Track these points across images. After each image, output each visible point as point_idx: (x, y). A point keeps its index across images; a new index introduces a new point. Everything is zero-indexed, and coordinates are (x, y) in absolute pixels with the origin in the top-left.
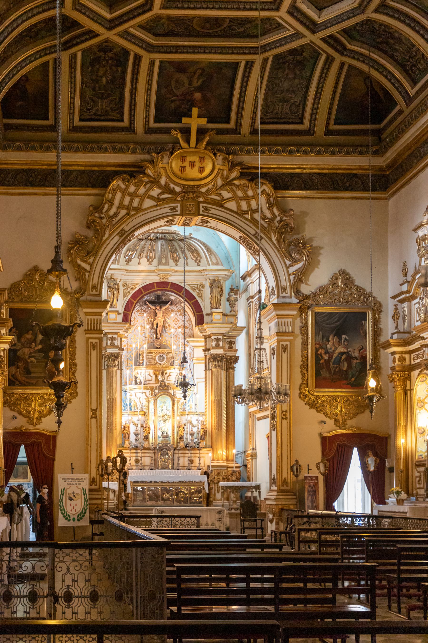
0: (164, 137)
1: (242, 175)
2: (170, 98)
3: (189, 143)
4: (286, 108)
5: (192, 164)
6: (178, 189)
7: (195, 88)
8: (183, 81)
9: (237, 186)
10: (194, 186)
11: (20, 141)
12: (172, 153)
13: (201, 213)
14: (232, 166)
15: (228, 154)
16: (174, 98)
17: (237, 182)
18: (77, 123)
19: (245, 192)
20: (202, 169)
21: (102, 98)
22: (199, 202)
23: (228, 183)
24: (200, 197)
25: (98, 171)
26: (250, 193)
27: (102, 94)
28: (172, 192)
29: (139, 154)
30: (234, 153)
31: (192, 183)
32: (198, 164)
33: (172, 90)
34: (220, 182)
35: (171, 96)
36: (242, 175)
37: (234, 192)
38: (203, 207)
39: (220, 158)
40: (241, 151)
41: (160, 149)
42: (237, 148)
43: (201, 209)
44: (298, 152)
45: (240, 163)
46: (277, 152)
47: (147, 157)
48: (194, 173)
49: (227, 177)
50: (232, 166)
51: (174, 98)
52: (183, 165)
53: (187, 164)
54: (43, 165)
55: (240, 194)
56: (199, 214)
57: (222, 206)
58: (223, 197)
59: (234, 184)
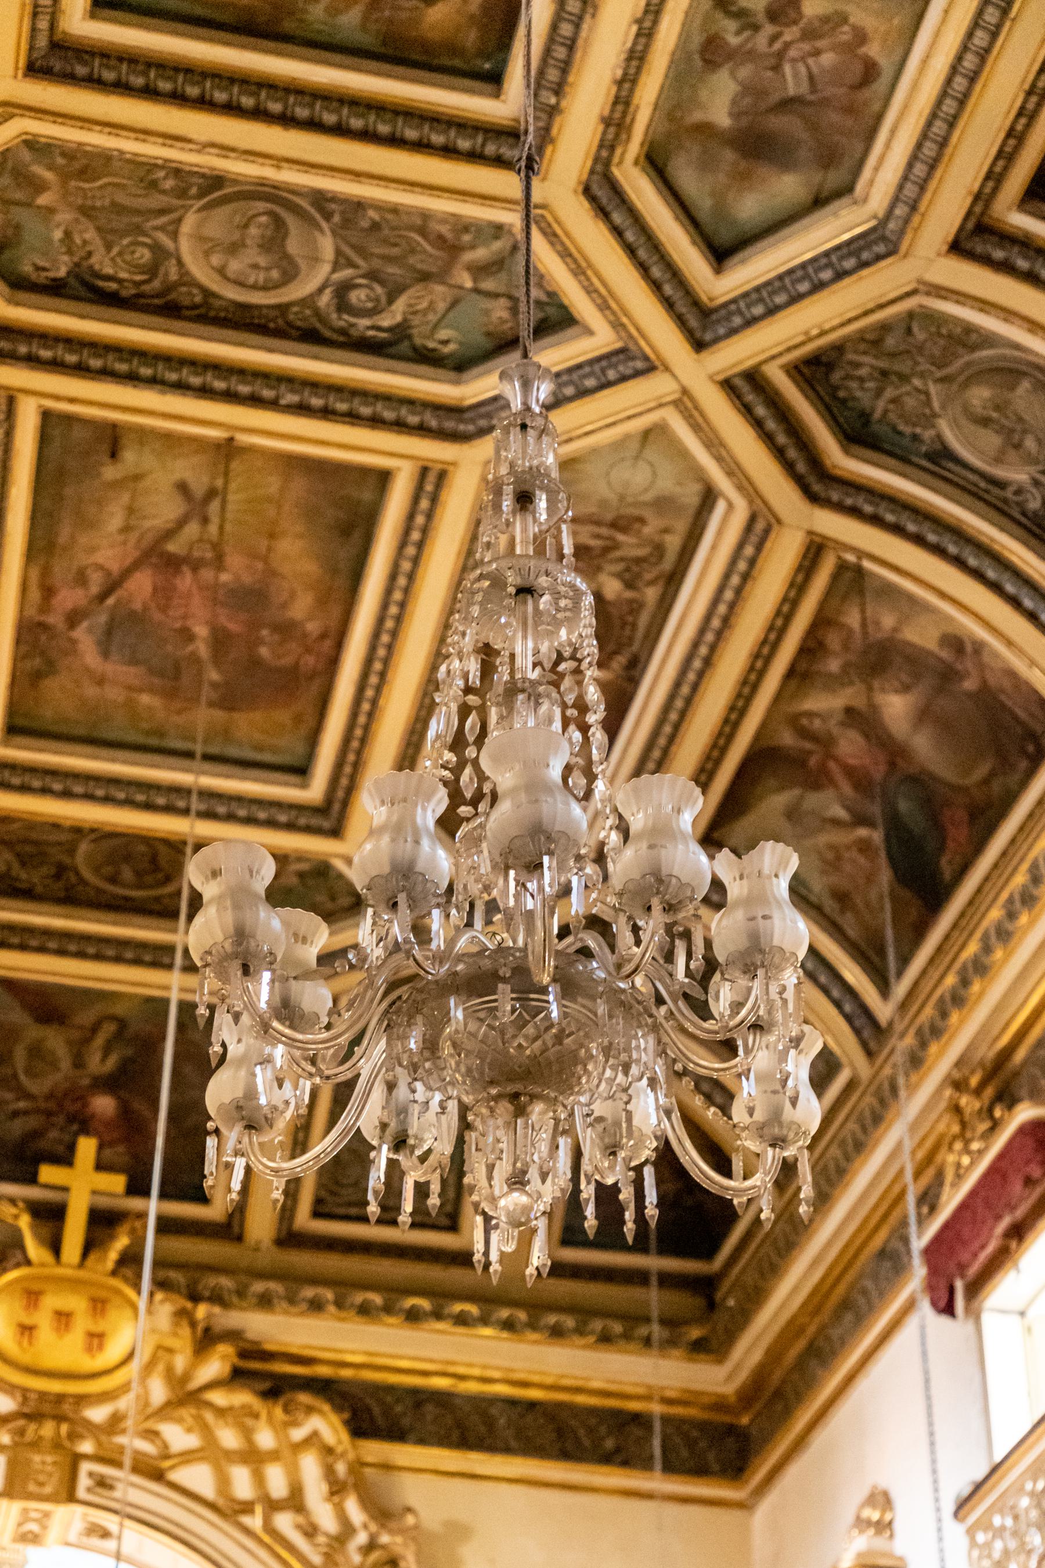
1: (238, 1376)
5: (63, 1318)
9: (221, 1412)
10: (60, 1398)
13: (81, 1493)
14: (206, 1340)
15: (195, 1298)
17: (219, 1398)
19: (247, 1434)
20: (96, 1340)
22: (77, 1459)
23: (186, 1398)
24: (81, 1437)
26: (265, 1439)
30: (217, 1298)
31: (56, 1387)
32: (82, 1324)
34: (158, 1392)
36: (238, 1376)
37: (206, 1432)
38: (91, 1474)
40: (241, 1293)
42: (226, 1282)
43: (84, 1482)
44: (438, 1315)
45: (233, 1336)
46: (365, 1310)
49: (186, 1377)
50: (206, 1340)
52: (27, 1321)
53: (43, 1319)
55: (229, 1438)
56: (71, 1497)
57: (158, 1476)
58: (166, 1446)
59: (209, 1405)
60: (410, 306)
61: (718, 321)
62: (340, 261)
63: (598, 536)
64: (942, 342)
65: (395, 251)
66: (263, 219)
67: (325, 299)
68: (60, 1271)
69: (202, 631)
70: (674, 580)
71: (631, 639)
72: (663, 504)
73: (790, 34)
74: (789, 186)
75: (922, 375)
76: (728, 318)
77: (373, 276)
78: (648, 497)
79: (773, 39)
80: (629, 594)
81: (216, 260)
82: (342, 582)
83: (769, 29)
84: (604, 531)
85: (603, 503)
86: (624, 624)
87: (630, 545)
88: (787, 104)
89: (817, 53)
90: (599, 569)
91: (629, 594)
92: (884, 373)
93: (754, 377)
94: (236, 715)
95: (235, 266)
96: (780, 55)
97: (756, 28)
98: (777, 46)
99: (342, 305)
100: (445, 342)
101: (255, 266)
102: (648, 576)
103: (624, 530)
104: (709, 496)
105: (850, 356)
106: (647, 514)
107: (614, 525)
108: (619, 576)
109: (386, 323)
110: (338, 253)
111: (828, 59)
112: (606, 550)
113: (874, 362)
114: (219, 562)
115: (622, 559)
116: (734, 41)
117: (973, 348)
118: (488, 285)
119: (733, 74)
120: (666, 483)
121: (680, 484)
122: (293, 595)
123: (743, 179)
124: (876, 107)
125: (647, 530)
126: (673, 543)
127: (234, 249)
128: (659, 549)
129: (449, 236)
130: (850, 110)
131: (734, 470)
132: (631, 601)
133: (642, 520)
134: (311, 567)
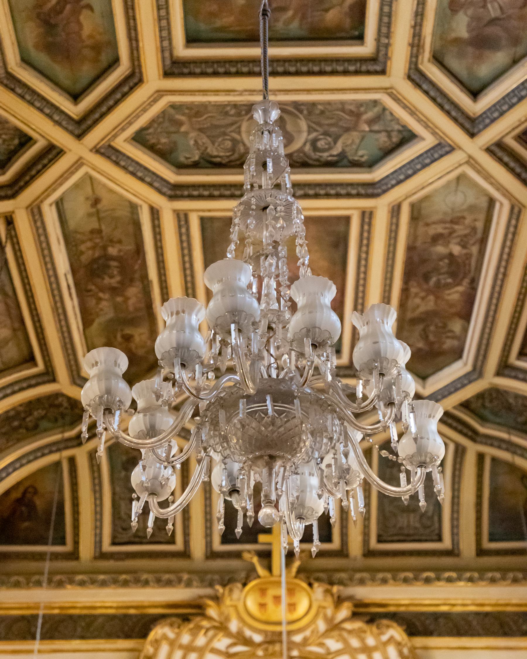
0: (234, 563)
3: (269, 568)
6: (258, 638)
11: (18, 574)
12: (245, 585)
18: (107, 547)
20: (292, 607)
25: (136, 616)
28: (248, 642)
29: (197, 587)
39: (319, 590)
41: (228, 580)
47: (208, 591)
48: (281, 613)
54: (53, 608)
61: (479, 123)
62: (311, 130)
63: (446, 228)
67: (308, 148)
68: (272, 579)
70: (483, 242)
71: (470, 271)
72: (472, 208)
74: (500, 58)
76: (483, 121)
77: (326, 134)
78: (465, 207)
80: (465, 251)
84: (448, 225)
85: (445, 213)
86: (465, 266)
87: (461, 230)
90: (449, 242)
91: (465, 251)
93: (500, 145)
99: (315, 148)
102: (471, 242)
103: (457, 223)
104: (492, 202)
106: (465, 214)
107: (452, 222)
108: (459, 244)
110: (309, 127)
112: (450, 234)
115: (458, 236)
118: (376, 128)
120: (471, 199)
123: (479, 58)
125: (467, 222)
126: (480, 225)
128: (474, 229)
131: (499, 187)
132: (466, 254)
133: (464, 218)
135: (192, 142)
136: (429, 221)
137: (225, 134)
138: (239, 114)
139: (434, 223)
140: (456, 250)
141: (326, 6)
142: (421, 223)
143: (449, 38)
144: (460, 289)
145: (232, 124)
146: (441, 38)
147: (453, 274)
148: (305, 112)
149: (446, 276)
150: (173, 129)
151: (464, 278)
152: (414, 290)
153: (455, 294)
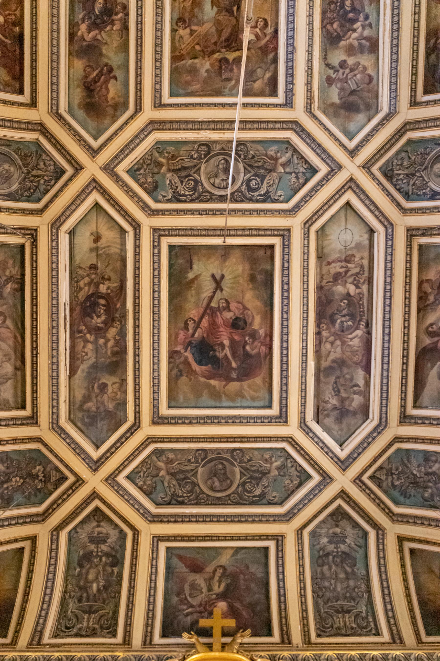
2: (184, 610)
4: (349, 619)
7: (217, 595)
8: (200, 586)
16: (190, 610)
21: (90, 612)
27: (91, 607)
33: (186, 599)
35: (185, 607)
51: (190, 610)
60: (268, 183)
63: (342, 267)
64: (420, 157)
65: (260, 164)
66: (223, 161)
67: (244, 188)
69: (226, 342)
70: (370, 281)
72: (358, 246)
73: (347, 71)
74: (361, 117)
75: (418, 171)
77: (256, 175)
78: (353, 245)
79: (343, 73)
80: (358, 291)
81: (212, 181)
82: (268, 309)
83: (341, 71)
84: (343, 264)
85: (340, 252)
88: (353, 92)
89: (355, 75)
91: (358, 291)
92: (407, 175)
94: (243, 383)
95: (217, 181)
96: (346, 78)
97: (338, 71)
98: (345, 76)
100: (280, 196)
101: (223, 180)
102: (362, 281)
105: (396, 172)
106: (354, 252)
108: (352, 283)
109: (262, 193)
110: (245, 168)
111: (359, 76)
112: (346, 272)
113: (403, 172)
114: (228, 308)
115: (352, 275)
116: (334, 76)
117: (429, 154)
118: (288, 170)
119: (336, 87)
121: (361, 236)
122: (253, 317)
123: (349, 119)
124: (376, 89)
125: (356, 260)
126: (365, 262)
127: (216, 176)
128: (362, 267)
129: (274, 155)
130: (369, 91)
132: (359, 294)
133: (353, 256)
134: (258, 303)
135: (168, 182)
136: (330, 259)
137: (189, 175)
138: (199, 158)
139: (333, 262)
140: (352, 289)
141: (255, 78)
142: (325, 263)
143: (328, 103)
144: (359, 333)
145: (195, 166)
146: (324, 103)
147: (352, 316)
148: (242, 156)
149: (348, 318)
150: (156, 170)
151: (360, 320)
152: (325, 334)
153: (355, 339)
